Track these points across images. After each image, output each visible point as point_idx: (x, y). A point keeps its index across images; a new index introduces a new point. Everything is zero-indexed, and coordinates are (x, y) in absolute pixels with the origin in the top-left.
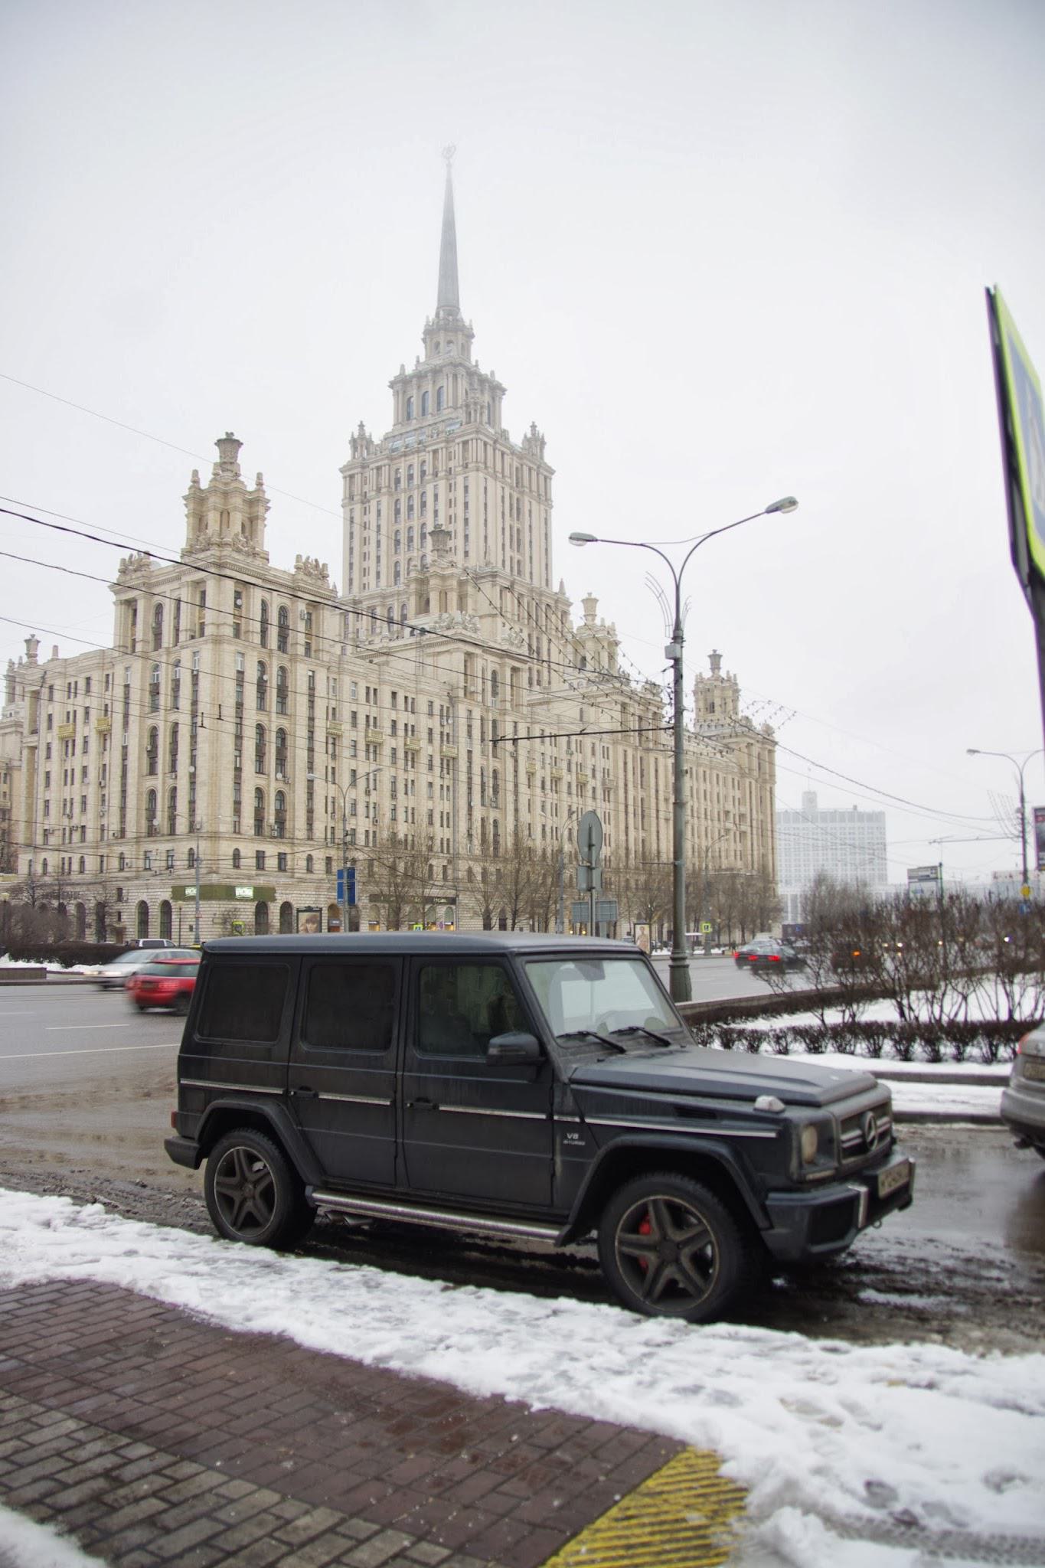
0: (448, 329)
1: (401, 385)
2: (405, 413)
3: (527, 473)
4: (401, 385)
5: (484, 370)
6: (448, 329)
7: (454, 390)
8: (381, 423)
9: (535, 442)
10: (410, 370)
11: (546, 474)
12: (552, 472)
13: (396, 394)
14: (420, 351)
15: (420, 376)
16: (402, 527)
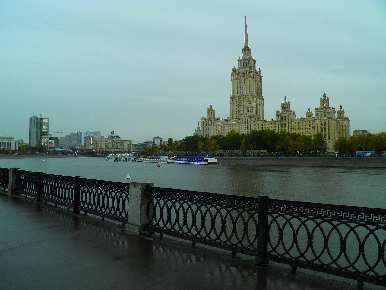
0: (247, 50)
1: (239, 61)
2: (240, 67)
3: (258, 76)
4: (239, 61)
5: (253, 58)
6: (247, 50)
8: (237, 68)
9: (260, 72)
10: (241, 58)
15: (243, 60)
16: (241, 85)
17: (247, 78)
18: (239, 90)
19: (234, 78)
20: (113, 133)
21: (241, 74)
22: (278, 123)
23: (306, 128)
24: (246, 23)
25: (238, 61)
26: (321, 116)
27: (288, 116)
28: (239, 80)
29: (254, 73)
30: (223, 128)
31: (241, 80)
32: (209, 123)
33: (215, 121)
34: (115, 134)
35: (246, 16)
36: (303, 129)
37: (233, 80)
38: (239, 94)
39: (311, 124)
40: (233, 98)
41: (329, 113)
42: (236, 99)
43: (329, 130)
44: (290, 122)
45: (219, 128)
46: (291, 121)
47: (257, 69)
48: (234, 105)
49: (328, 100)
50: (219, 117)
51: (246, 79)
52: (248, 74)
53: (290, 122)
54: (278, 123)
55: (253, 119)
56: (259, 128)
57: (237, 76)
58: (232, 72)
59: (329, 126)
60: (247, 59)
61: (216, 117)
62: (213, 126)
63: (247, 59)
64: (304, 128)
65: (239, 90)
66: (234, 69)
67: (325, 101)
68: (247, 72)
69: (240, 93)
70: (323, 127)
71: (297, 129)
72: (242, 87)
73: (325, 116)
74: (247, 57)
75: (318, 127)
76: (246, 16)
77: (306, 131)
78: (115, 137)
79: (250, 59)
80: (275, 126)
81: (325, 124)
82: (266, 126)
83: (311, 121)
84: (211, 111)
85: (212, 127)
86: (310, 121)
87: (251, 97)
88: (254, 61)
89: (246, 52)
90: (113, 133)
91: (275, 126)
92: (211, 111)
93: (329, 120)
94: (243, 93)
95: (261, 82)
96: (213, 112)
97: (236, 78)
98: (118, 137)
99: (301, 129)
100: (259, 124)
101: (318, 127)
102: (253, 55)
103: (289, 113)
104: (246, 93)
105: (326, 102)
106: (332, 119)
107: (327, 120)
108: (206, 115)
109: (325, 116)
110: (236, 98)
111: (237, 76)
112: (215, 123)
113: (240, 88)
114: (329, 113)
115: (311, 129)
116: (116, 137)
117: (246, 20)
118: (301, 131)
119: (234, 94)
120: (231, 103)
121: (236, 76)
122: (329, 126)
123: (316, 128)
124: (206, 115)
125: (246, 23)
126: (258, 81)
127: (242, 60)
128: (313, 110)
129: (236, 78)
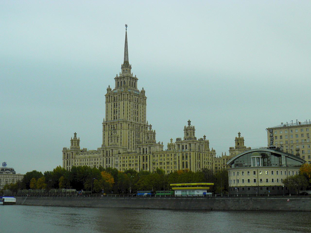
0: (126, 66)
1: (117, 79)
2: (118, 85)
4: (117, 79)
5: (134, 76)
6: (126, 66)
7: (127, 81)
8: (113, 87)
9: (143, 92)
10: (119, 76)
11: (145, 98)
12: (146, 98)
13: (116, 81)
14: (120, 71)
15: (120, 78)
16: (115, 109)
17: (121, 100)
18: (112, 114)
19: (108, 100)
20: (5, 164)
21: (116, 96)
22: (140, 156)
23: (168, 163)
24: (126, 33)
25: (115, 79)
26: (183, 148)
27: (150, 148)
28: (113, 103)
29: (130, 94)
30: (134, 159)
31: (116, 103)
32: (146, 152)
33: (77, 154)
34: (8, 166)
35: (126, 26)
36: (164, 163)
37: (107, 102)
38: (112, 119)
39: (173, 157)
40: (105, 124)
41: (190, 144)
42: (110, 127)
43: (190, 165)
44: (151, 155)
45: (81, 162)
46: (153, 154)
47: (139, 88)
48: (107, 133)
49: (193, 129)
50: (85, 148)
51: (120, 102)
52: (123, 95)
53: (151, 155)
54: (140, 156)
55: (115, 152)
56: (120, 161)
57: (112, 98)
58: (106, 92)
59: (190, 160)
60: (125, 77)
61: (81, 148)
62: (74, 159)
63: (124, 77)
64: (165, 162)
65: (112, 114)
66: (109, 89)
67: (189, 130)
68: (121, 94)
69: (114, 119)
70: (185, 161)
71: (158, 163)
72: (117, 112)
73: (186, 148)
74: (125, 75)
75: (179, 161)
76: (126, 26)
77: (168, 166)
78: (7, 169)
79: (127, 77)
80: (136, 159)
81: (187, 157)
82: (165, 158)
83: (173, 154)
84: (75, 141)
85: (73, 160)
86: (171, 154)
87: (125, 123)
88: (136, 79)
89: (125, 69)
90: (5, 164)
91: (136, 159)
92: (75, 141)
93: (190, 153)
94: (117, 118)
95: (144, 104)
96: (76, 142)
97: (110, 100)
98: (12, 170)
99: (163, 164)
100: (120, 158)
101: (179, 161)
102: (134, 72)
103: (150, 145)
104: (120, 118)
105: (189, 131)
106: (193, 151)
107: (189, 153)
108: (68, 146)
109: (186, 148)
110: (109, 125)
111: (112, 98)
112: (77, 156)
113: (114, 112)
114: (190, 144)
115: (173, 163)
116: (8, 170)
117: (126, 29)
118: (163, 166)
119: (108, 120)
120: (104, 130)
121: (111, 97)
122: (190, 160)
123: (177, 162)
124: (68, 146)
125: (126, 33)
126: (139, 104)
127: (119, 78)
128: (174, 141)
129: (110, 100)
